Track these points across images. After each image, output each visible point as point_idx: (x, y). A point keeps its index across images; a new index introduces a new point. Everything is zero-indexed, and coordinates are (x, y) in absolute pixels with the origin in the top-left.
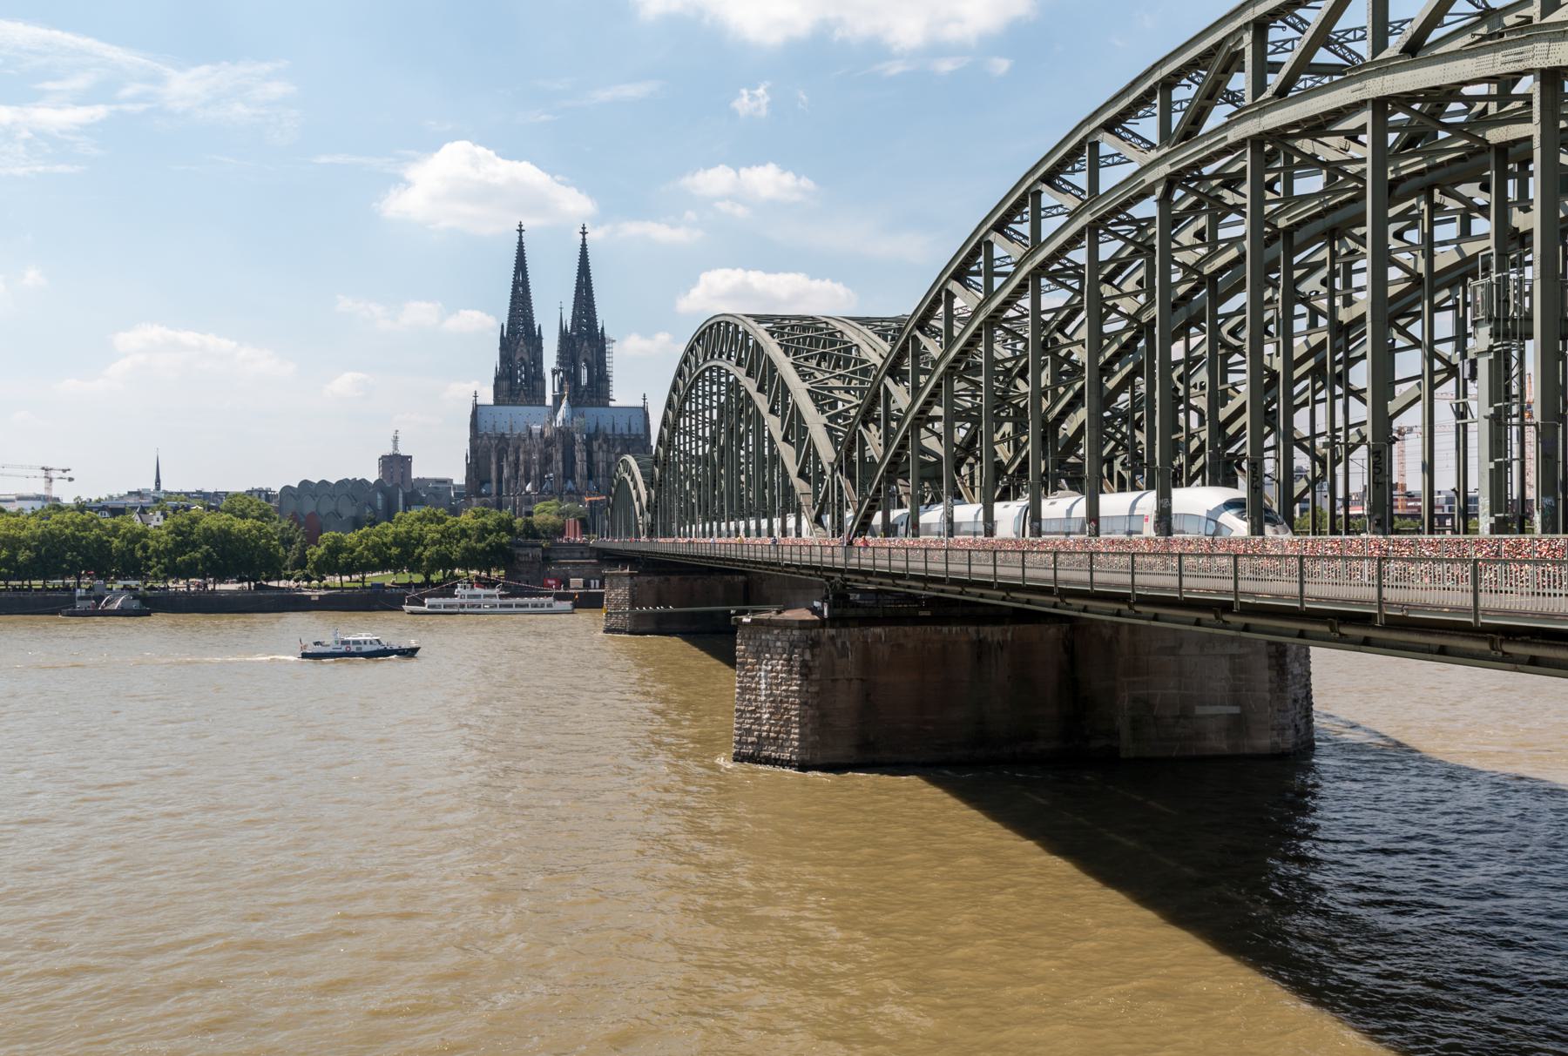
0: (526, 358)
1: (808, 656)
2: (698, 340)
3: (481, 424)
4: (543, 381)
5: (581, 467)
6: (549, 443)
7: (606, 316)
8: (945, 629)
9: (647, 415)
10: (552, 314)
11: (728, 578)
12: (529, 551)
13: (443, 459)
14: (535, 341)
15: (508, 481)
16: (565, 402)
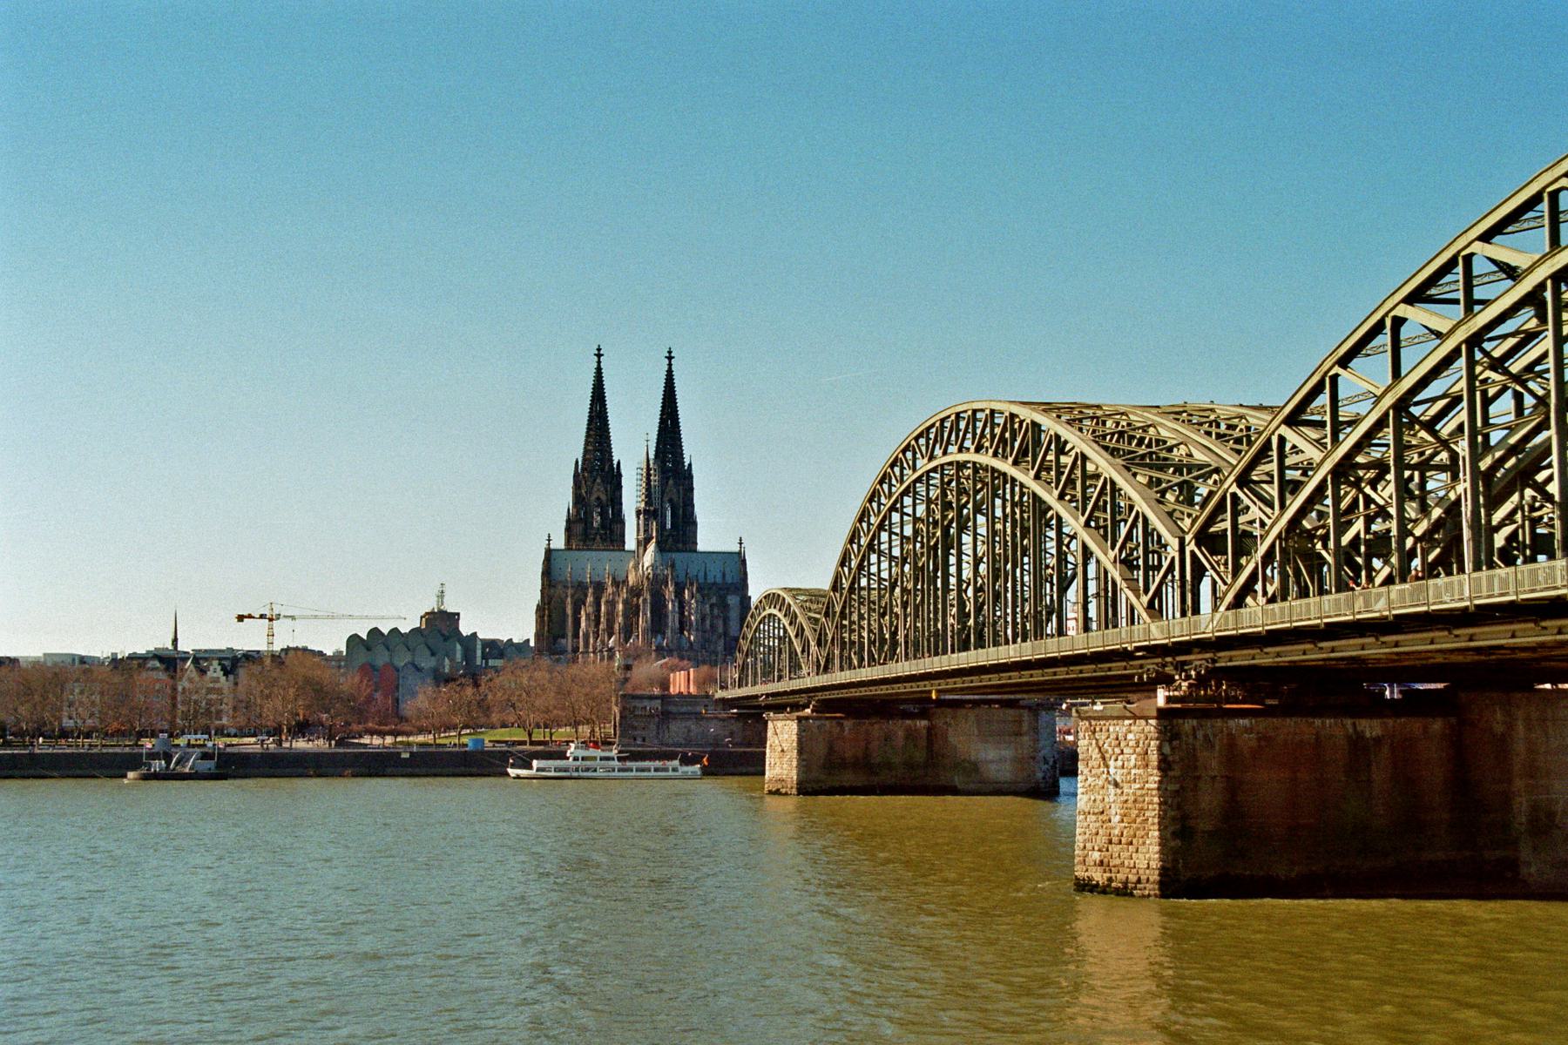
0: (603, 497)
1: (1167, 750)
2: (916, 439)
3: (555, 573)
4: (622, 523)
5: (672, 620)
6: (636, 592)
7: (691, 450)
8: (1318, 722)
9: (744, 562)
10: (632, 449)
11: (908, 722)
12: (646, 703)
13: (505, 613)
14: (613, 478)
15: (586, 636)
16: (652, 547)
